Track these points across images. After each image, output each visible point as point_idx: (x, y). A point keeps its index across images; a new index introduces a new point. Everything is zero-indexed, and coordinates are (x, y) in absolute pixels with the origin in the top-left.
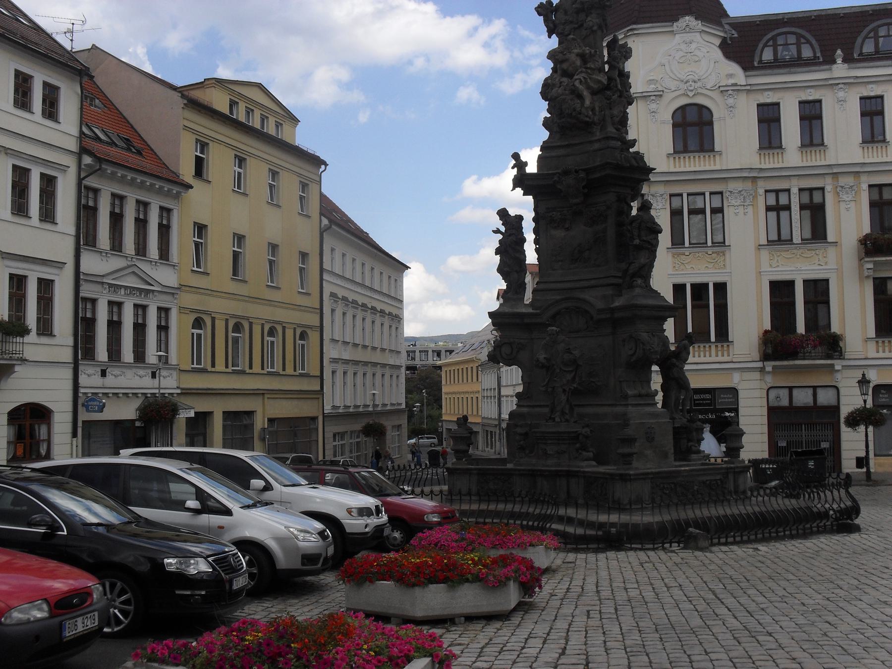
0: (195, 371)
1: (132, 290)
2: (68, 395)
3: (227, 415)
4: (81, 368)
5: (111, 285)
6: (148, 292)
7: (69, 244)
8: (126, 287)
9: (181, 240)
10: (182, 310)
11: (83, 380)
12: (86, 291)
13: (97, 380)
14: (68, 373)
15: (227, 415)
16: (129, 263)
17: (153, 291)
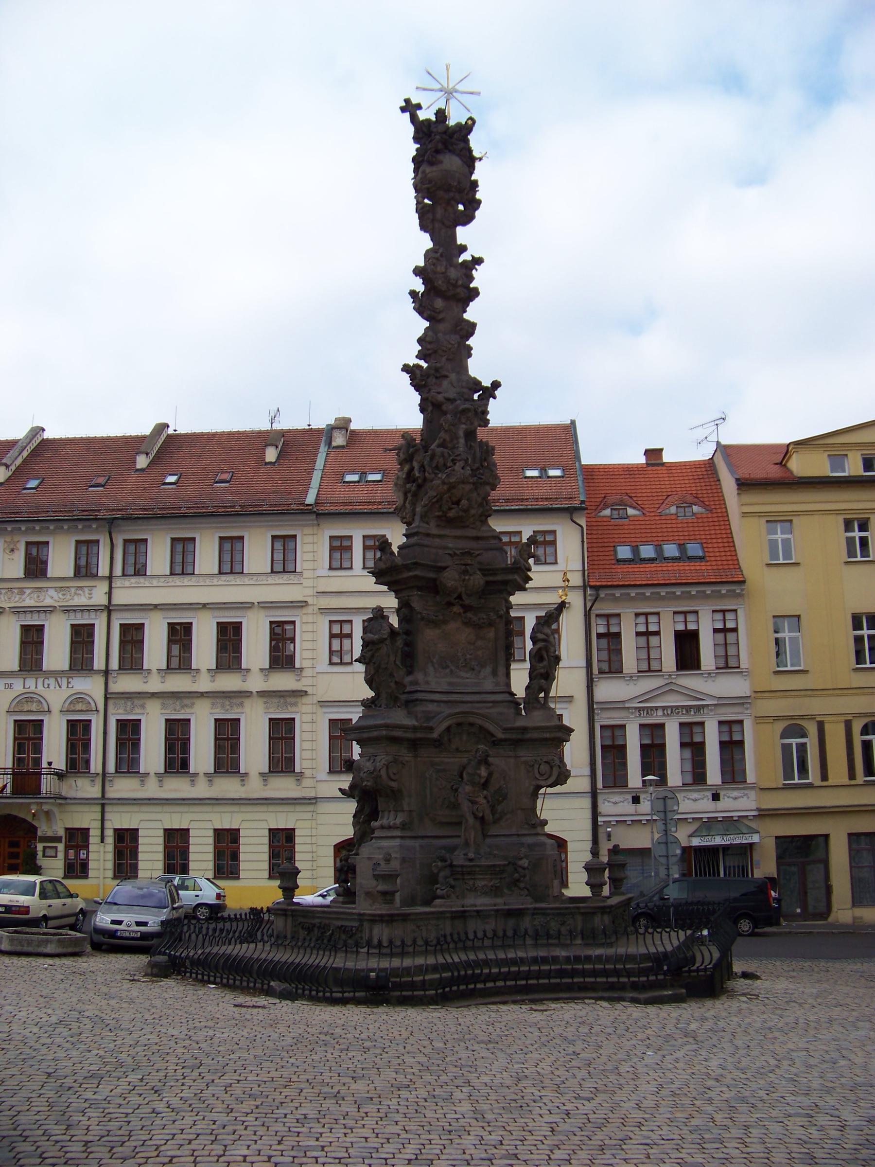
0: (786, 787)
1: (675, 710)
2: (588, 825)
3: (853, 837)
4: (600, 799)
5: (640, 709)
6: (699, 708)
7: (582, 675)
8: (664, 708)
9: (754, 644)
10: (759, 720)
11: (605, 807)
12: (604, 719)
13: (627, 807)
14: (587, 802)
15: (853, 837)
16: (667, 682)
17: (707, 705)
